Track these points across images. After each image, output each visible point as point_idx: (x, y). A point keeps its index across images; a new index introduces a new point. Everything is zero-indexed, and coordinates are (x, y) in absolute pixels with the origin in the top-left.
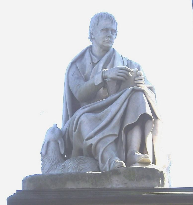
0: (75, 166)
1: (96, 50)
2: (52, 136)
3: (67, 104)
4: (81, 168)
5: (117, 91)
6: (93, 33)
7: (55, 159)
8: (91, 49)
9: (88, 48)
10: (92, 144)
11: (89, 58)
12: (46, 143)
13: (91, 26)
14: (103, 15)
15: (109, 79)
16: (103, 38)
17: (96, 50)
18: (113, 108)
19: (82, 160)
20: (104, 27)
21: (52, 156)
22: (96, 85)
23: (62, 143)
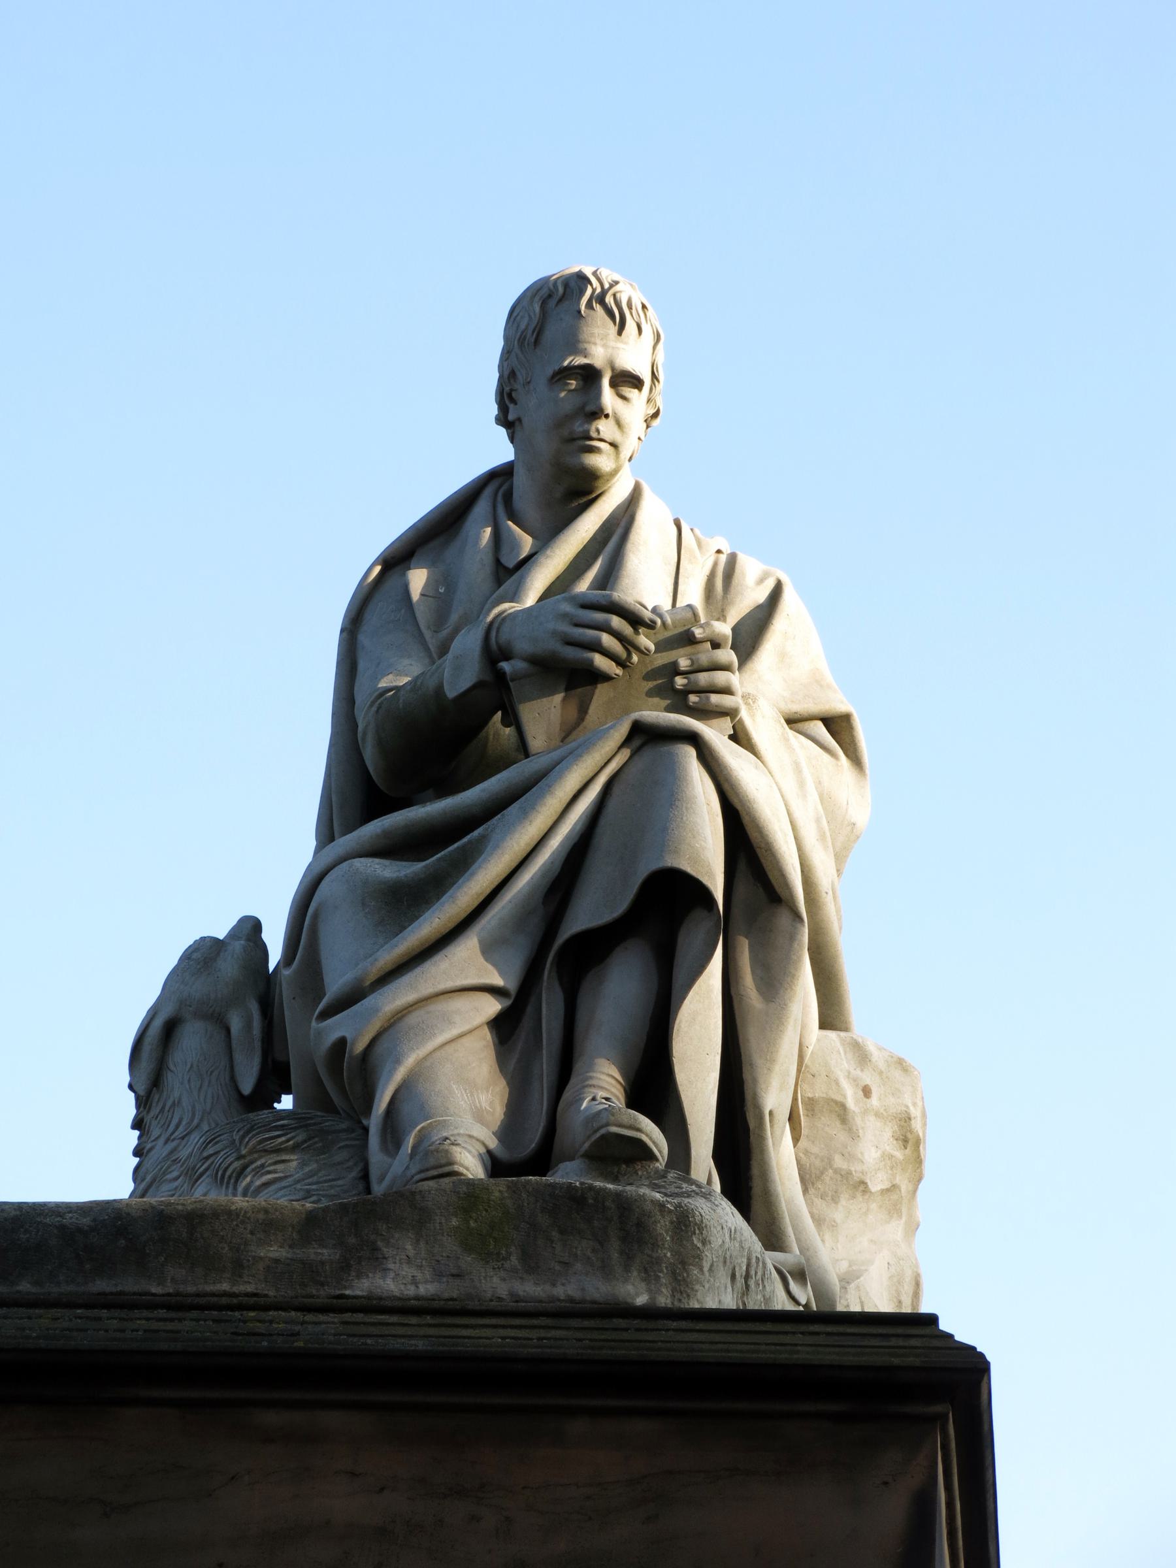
3: (334, 799)
6: (511, 390)
7: (196, 1122)
8: (504, 488)
12: (158, 1023)
14: (572, 284)
19: (277, 1128)
22: (451, 693)
23: (248, 1026)
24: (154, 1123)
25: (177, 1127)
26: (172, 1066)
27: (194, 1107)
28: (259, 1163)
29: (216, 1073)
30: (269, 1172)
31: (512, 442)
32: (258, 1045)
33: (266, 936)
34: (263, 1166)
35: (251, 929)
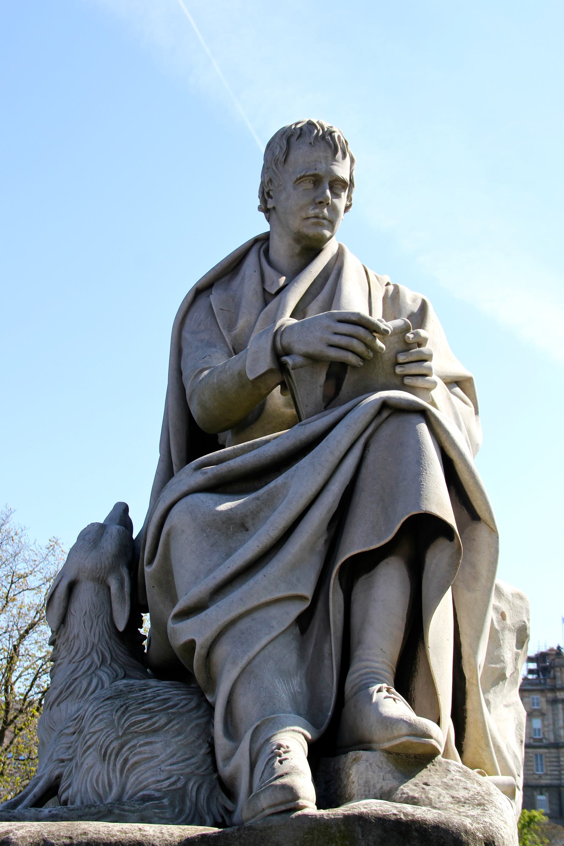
0: (112, 747)
1: (281, 249)
2: (89, 562)
3: (170, 430)
4: (135, 755)
5: (329, 402)
6: (269, 190)
7: (88, 650)
8: (264, 247)
9: (256, 240)
10: (191, 644)
11: (256, 277)
13: (266, 169)
15: (299, 360)
16: (302, 208)
17: (281, 249)
18: (299, 482)
20: (303, 170)
21: (82, 636)
22: (251, 377)
24: (62, 647)
25: (77, 653)
26: (73, 611)
27: (87, 640)
28: (132, 743)
29: (101, 617)
30: (140, 753)
31: (268, 221)
32: (127, 598)
33: (132, 514)
34: (134, 746)
35: (122, 513)
